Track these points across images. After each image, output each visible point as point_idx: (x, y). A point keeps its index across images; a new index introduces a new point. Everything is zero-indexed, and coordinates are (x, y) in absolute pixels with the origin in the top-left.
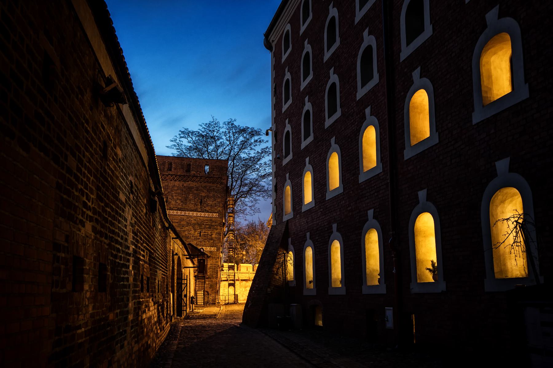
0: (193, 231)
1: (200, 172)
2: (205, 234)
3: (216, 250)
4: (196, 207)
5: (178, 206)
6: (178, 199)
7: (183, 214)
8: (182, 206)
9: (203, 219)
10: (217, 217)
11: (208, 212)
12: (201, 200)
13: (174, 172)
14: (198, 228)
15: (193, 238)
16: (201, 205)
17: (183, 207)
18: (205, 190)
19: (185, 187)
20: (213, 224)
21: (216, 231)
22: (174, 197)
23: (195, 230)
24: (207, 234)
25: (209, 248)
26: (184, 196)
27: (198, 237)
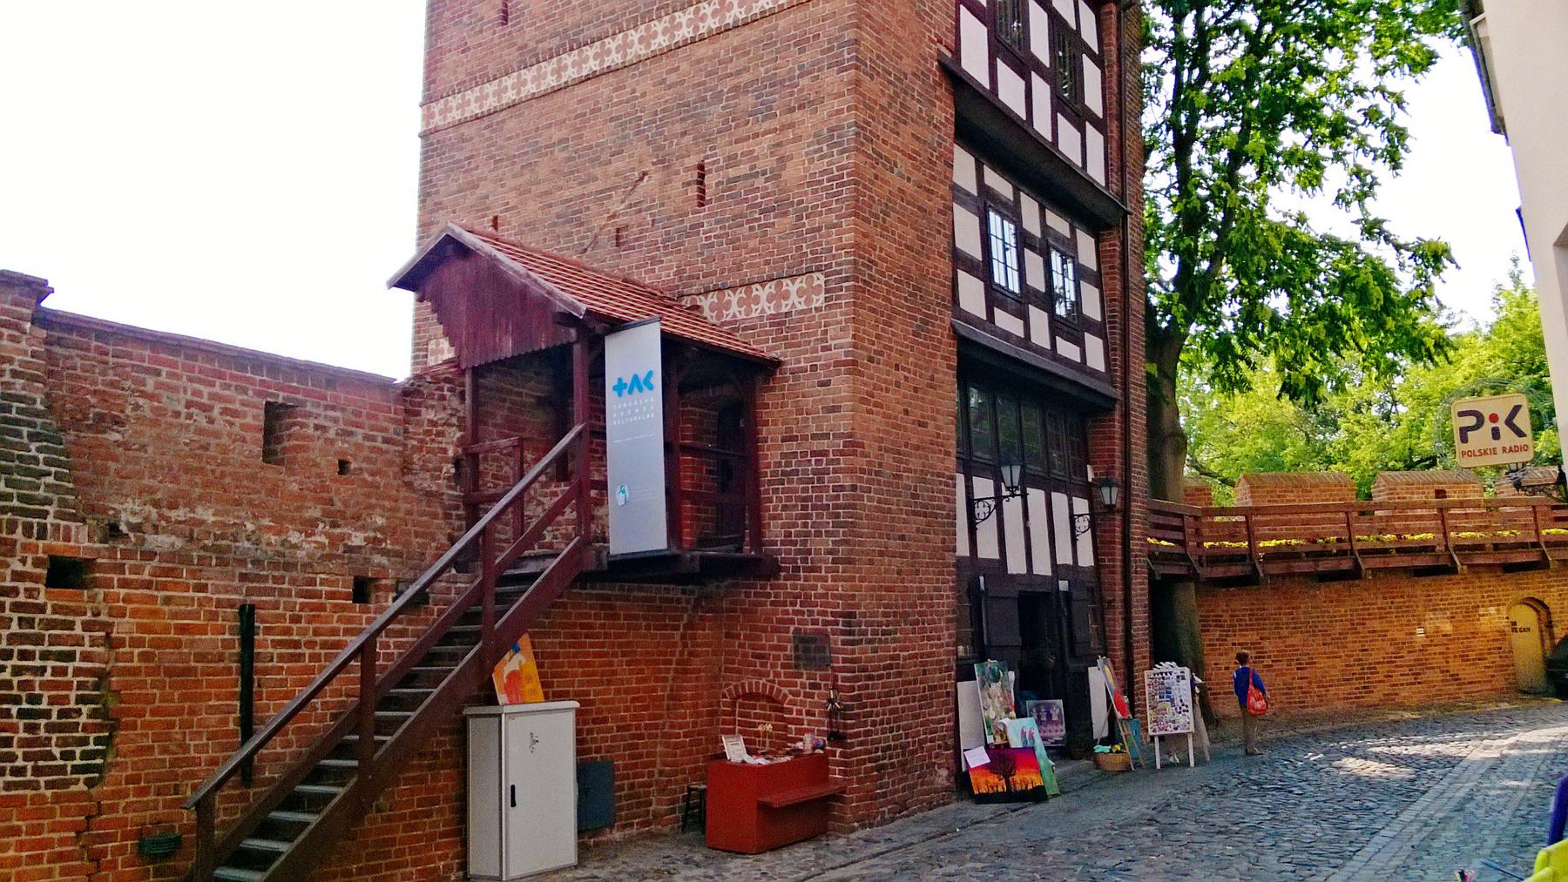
0: (656, 177)
2: (732, 172)
3: (819, 300)
5: (562, 19)
9: (716, 56)
14: (687, 139)
20: (791, 62)
21: (808, 122)
23: (664, 162)
24: (744, 169)
25: (770, 288)
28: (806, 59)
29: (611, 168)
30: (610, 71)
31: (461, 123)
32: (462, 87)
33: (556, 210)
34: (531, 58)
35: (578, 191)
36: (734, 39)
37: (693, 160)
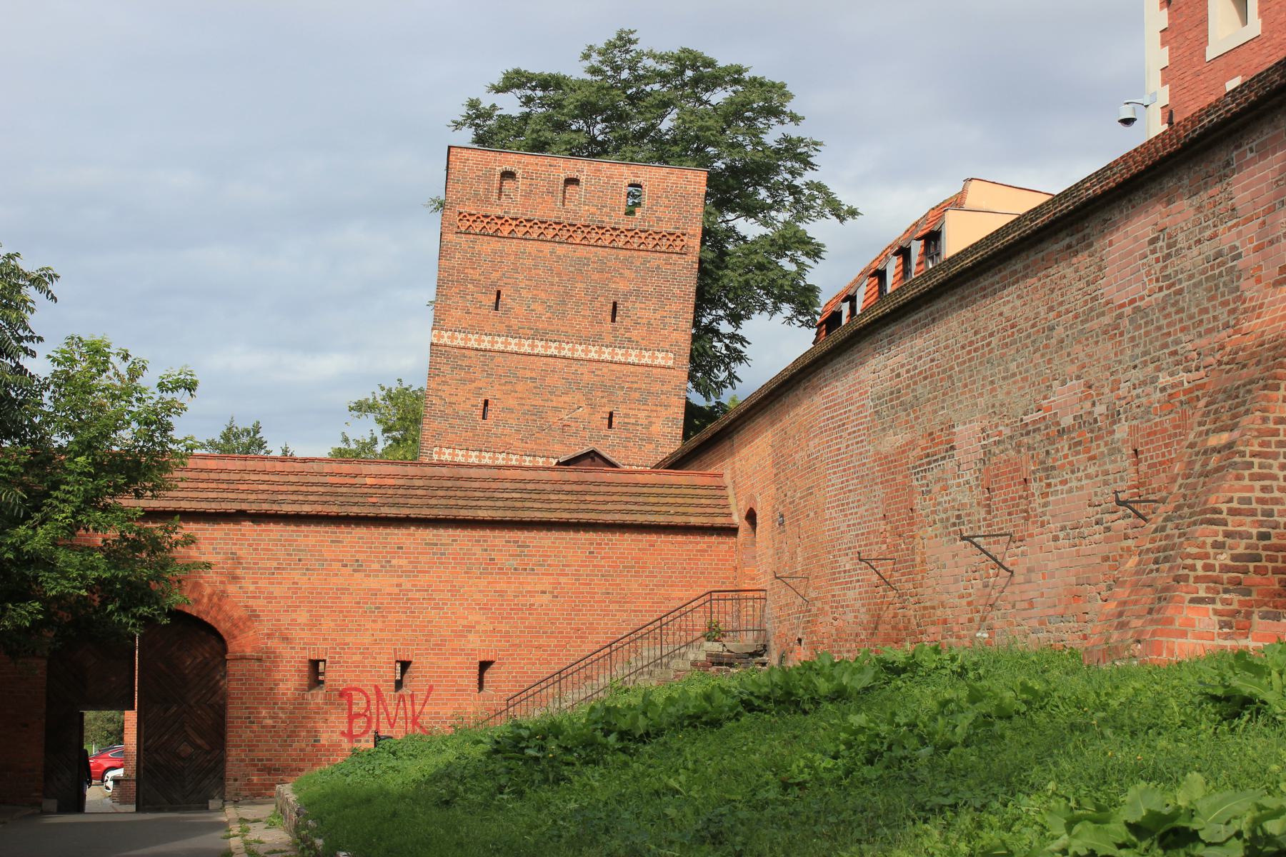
1: (613, 209)
2: (626, 420)
4: (597, 329)
6: (534, 299)
7: (553, 350)
8: (550, 323)
10: (670, 363)
11: (637, 346)
12: (615, 304)
13: (523, 205)
14: (605, 400)
15: (587, 434)
16: (613, 320)
17: (551, 328)
18: (627, 273)
19: (559, 257)
20: (657, 387)
22: (524, 293)
24: (633, 421)
26: (556, 287)
27: (602, 433)
28: (665, 388)
29: (560, 399)
30: (564, 358)
31: (464, 348)
32: (464, 331)
33: (526, 407)
34: (511, 333)
35: (542, 403)
36: (632, 368)
37: (608, 409)
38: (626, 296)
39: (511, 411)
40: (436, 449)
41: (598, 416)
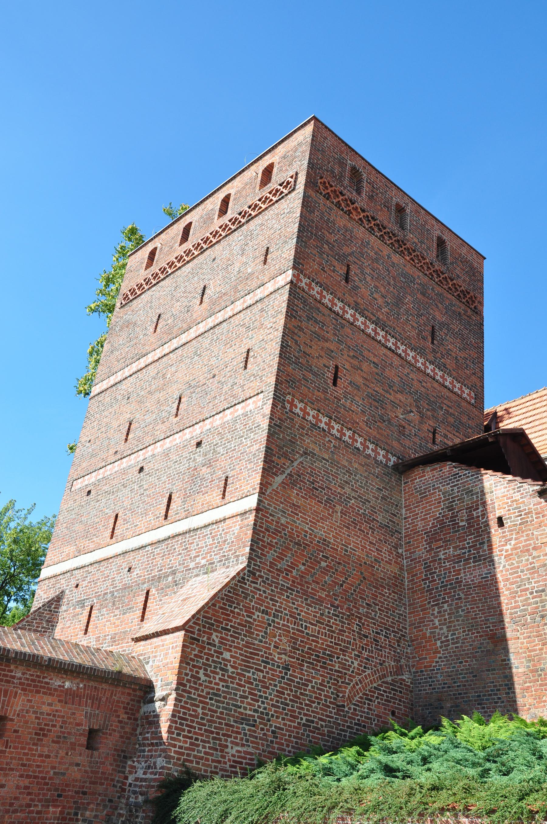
16: (432, 343)
22: (368, 278)
33: (370, 390)
35: (381, 391)
38: (443, 325)
39: (358, 388)
40: (289, 398)
41: (425, 427)
